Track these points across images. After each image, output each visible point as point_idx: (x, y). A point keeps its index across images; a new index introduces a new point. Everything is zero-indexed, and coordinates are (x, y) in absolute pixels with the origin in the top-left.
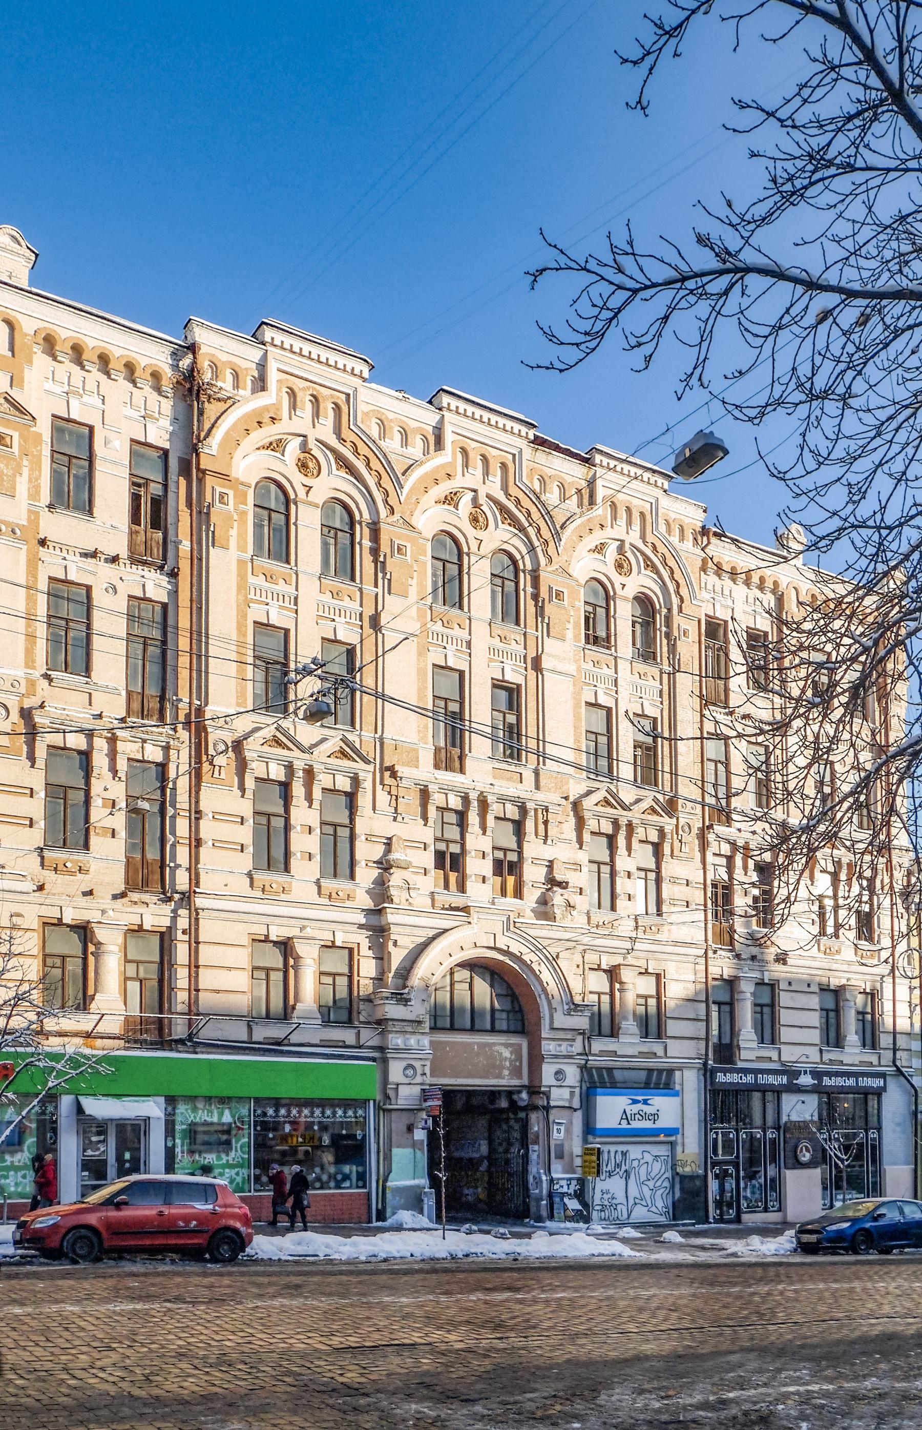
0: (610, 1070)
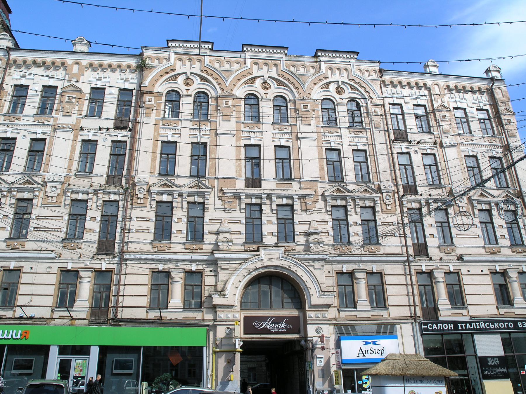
0: (352, 326)
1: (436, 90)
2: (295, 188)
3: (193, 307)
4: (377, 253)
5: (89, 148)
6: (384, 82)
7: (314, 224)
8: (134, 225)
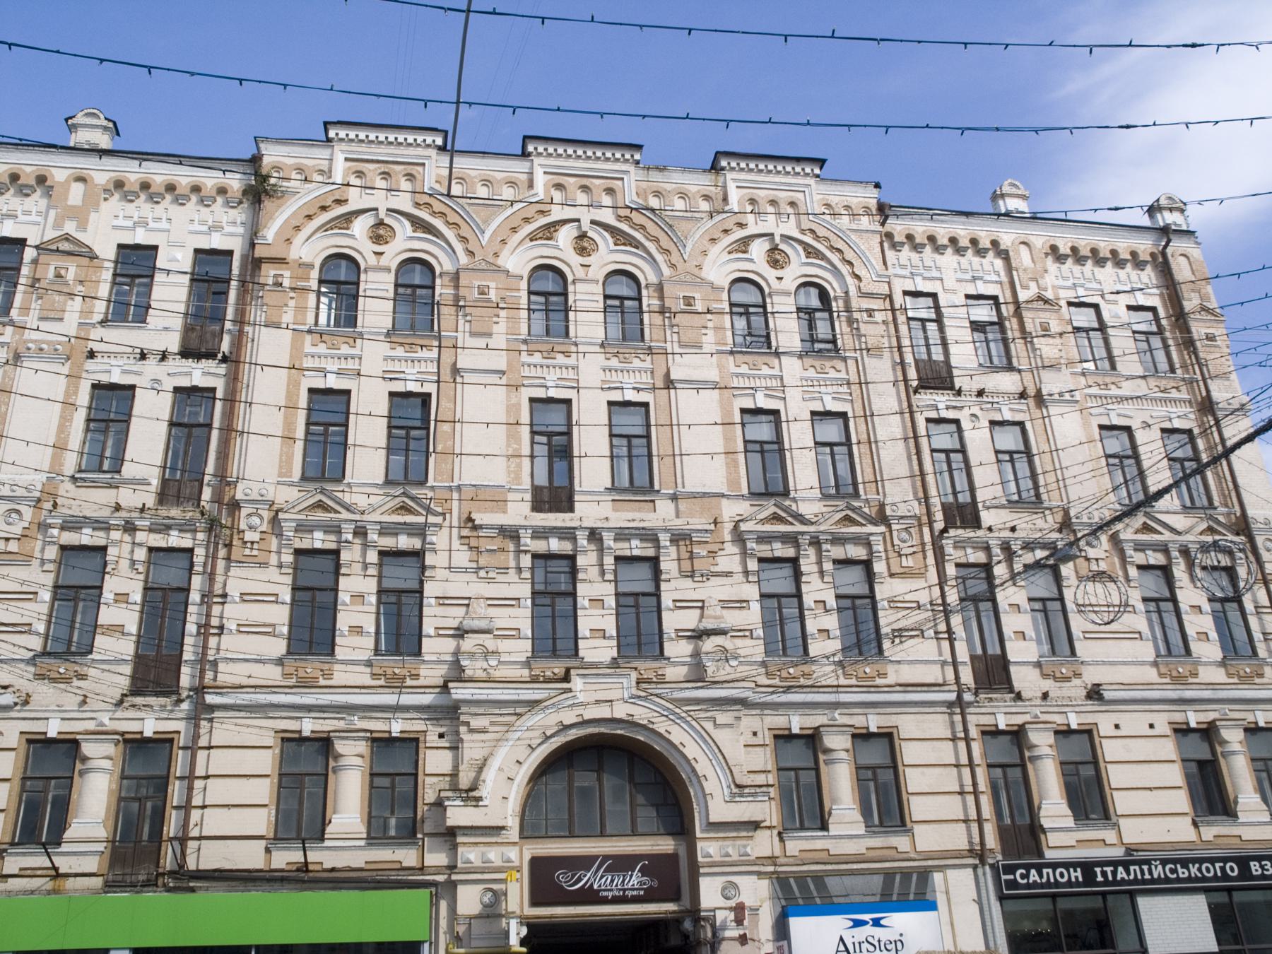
0: (819, 879)
1: (1023, 258)
2: (662, 514)
3: (393, 833)
4: (879, 681)
5: (111, 407)
6: (889, 236)
7: (714, 610)
8: (234, 613)
